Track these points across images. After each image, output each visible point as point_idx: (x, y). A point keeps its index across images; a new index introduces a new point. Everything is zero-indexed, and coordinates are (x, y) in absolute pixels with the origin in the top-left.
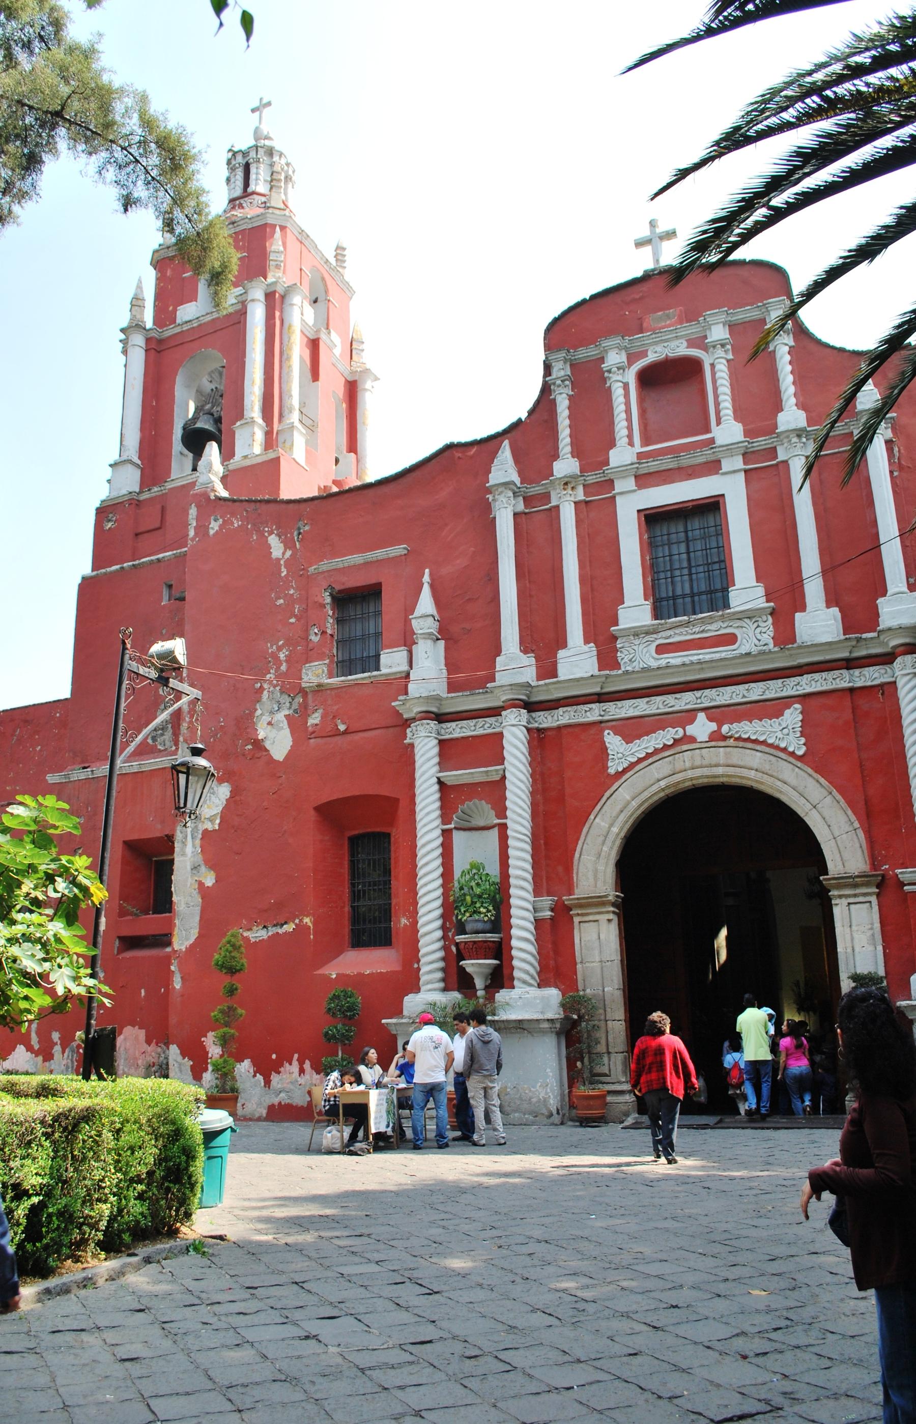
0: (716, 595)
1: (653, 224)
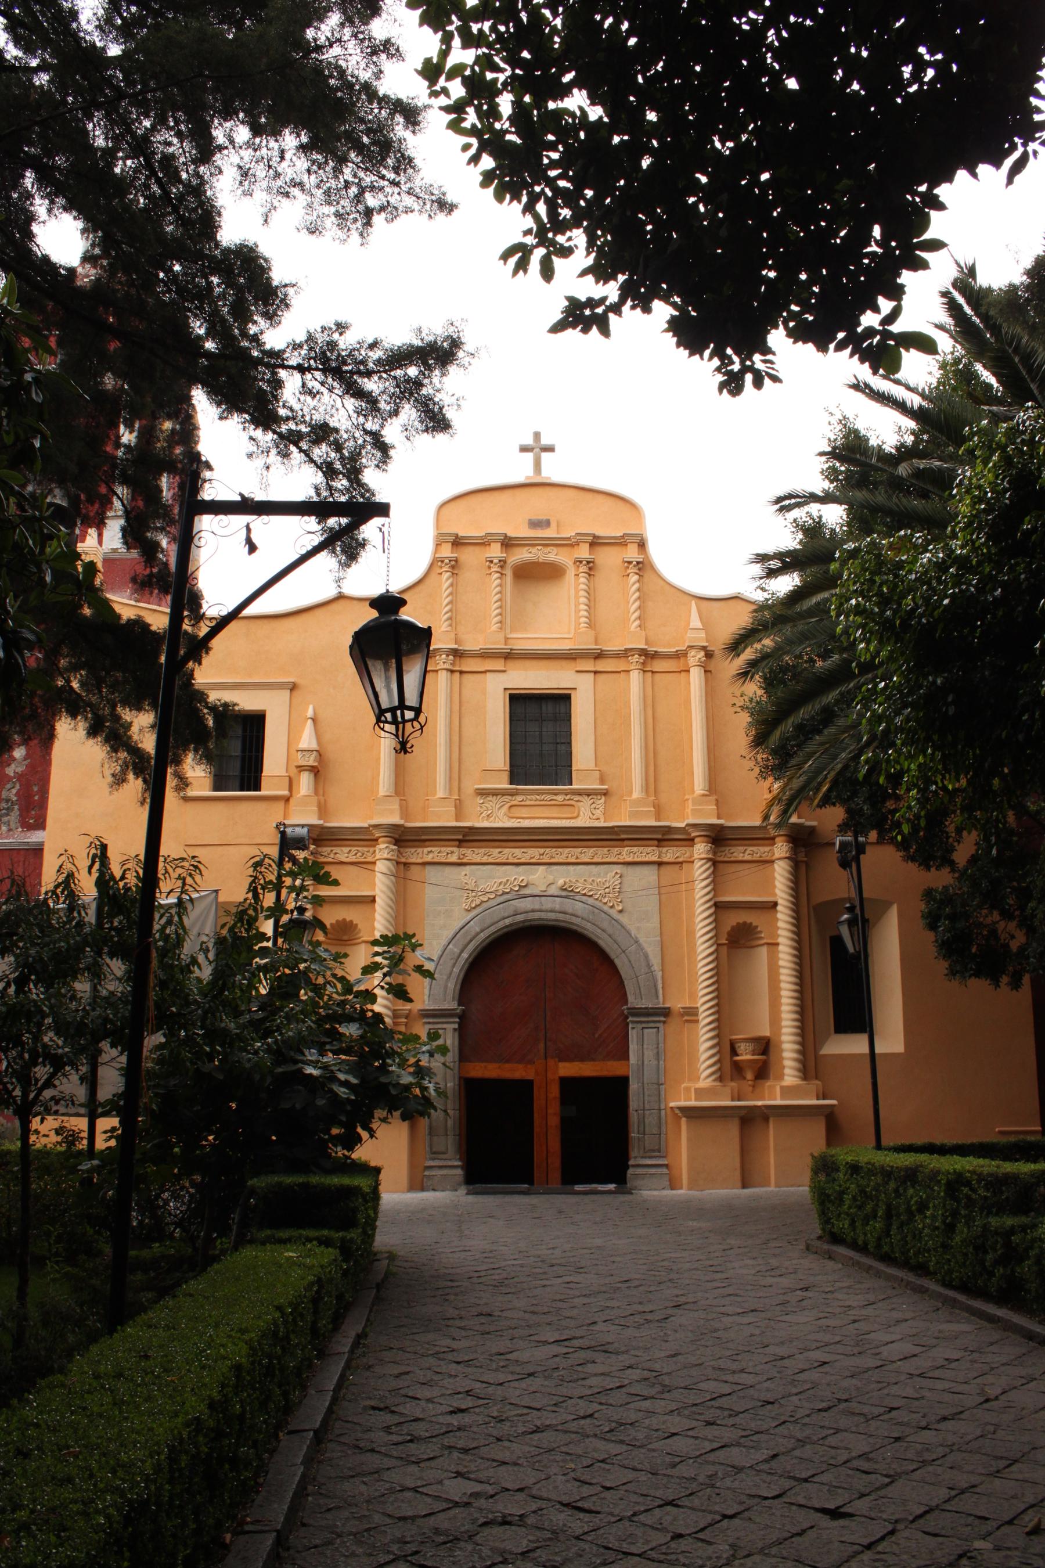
1: (537, 436)
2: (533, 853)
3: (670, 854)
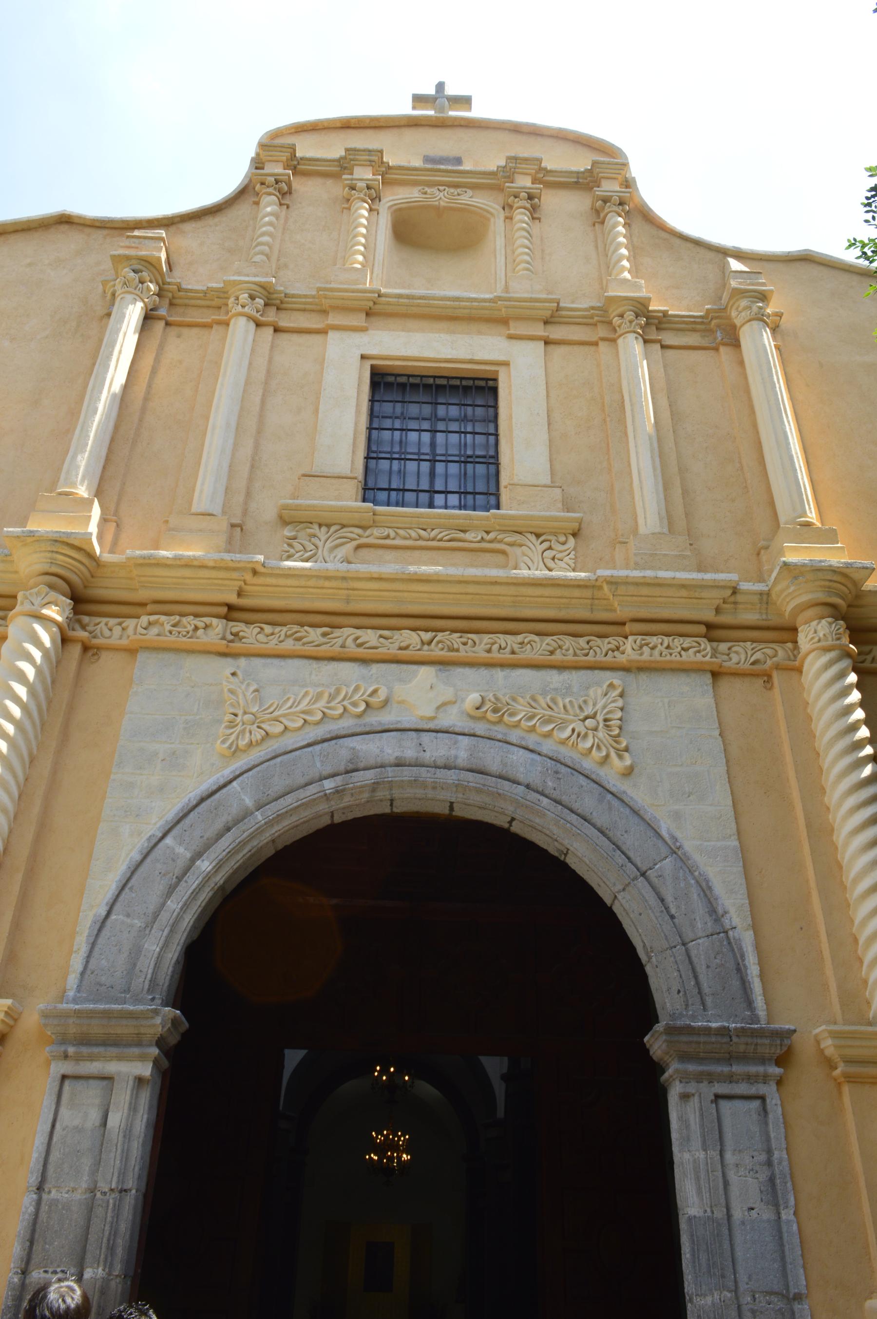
2: (412, 638)
3: (740, 655)
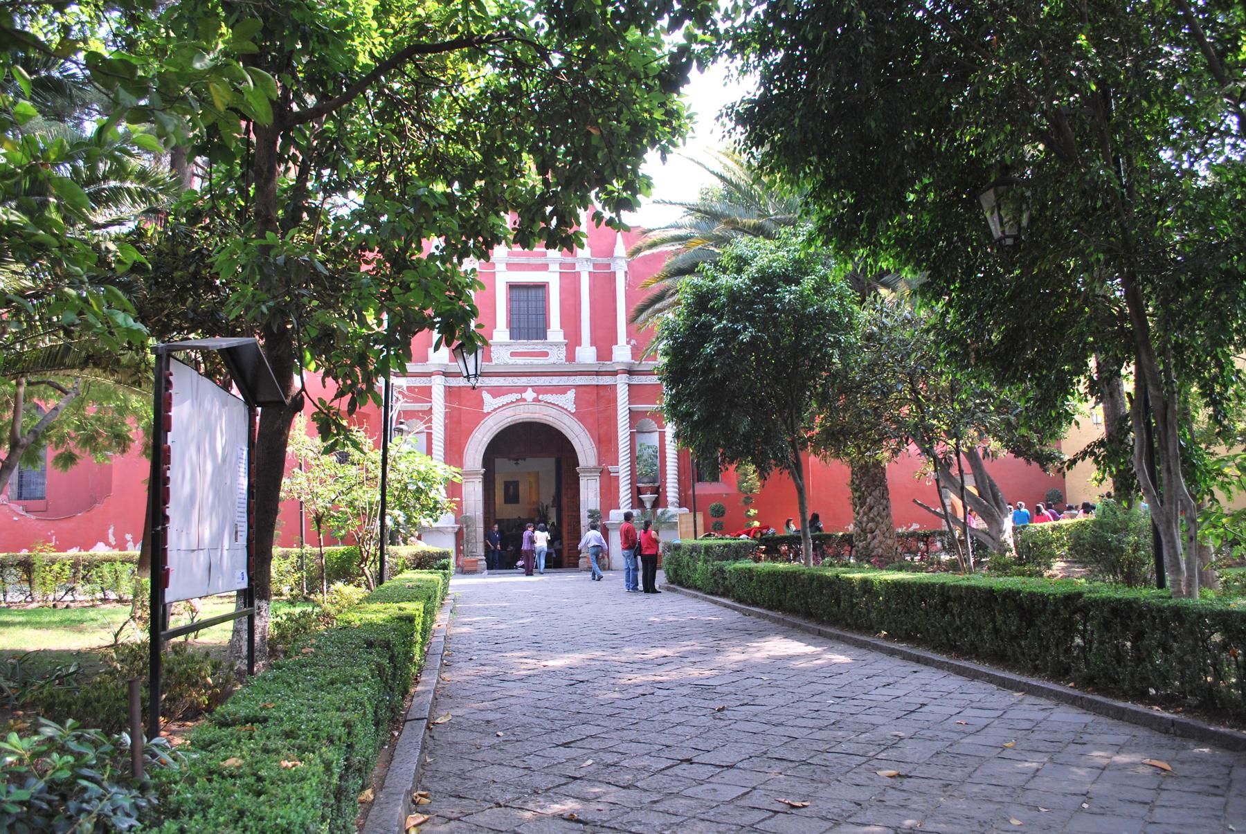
0: (540, 332)
